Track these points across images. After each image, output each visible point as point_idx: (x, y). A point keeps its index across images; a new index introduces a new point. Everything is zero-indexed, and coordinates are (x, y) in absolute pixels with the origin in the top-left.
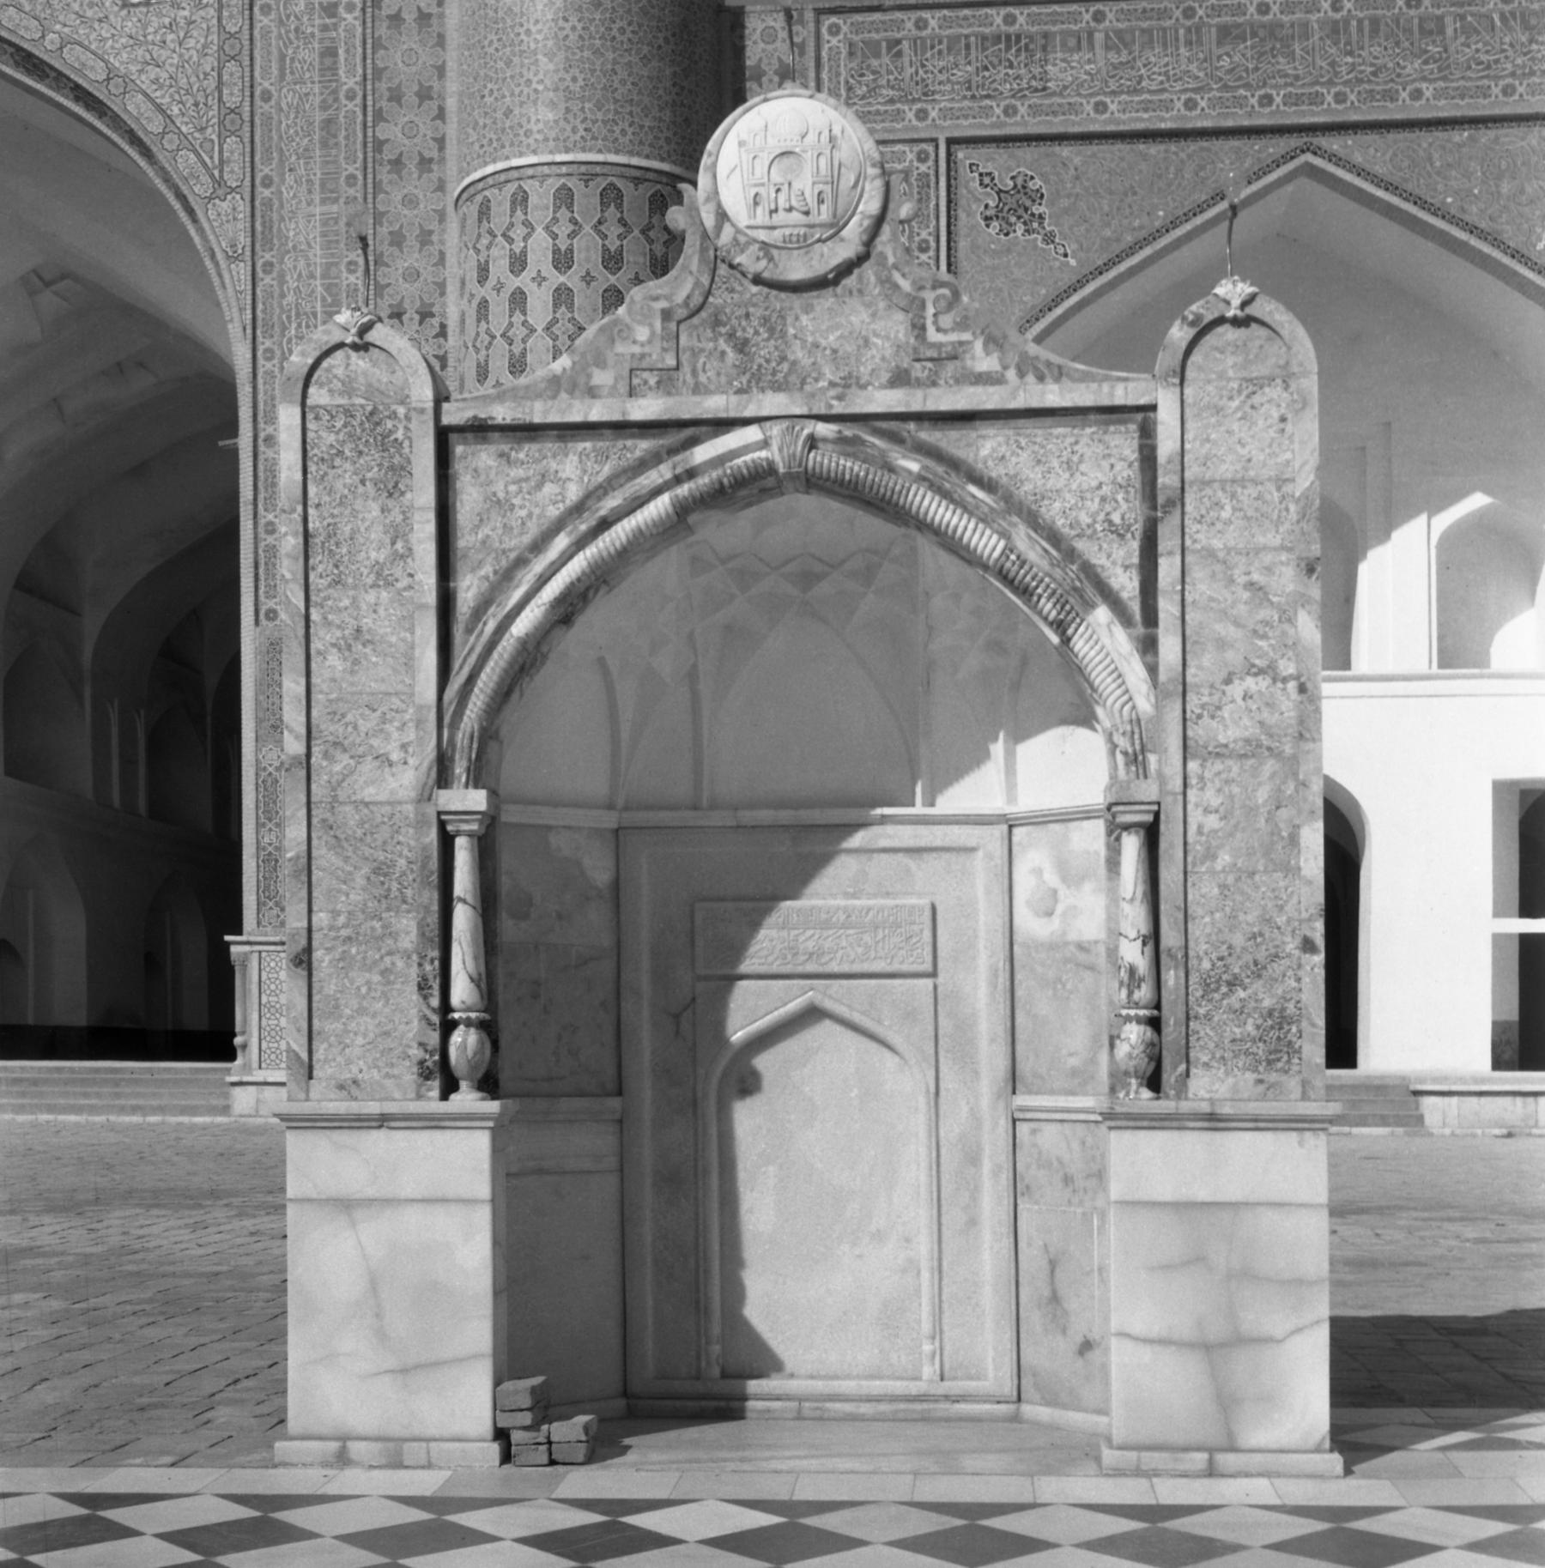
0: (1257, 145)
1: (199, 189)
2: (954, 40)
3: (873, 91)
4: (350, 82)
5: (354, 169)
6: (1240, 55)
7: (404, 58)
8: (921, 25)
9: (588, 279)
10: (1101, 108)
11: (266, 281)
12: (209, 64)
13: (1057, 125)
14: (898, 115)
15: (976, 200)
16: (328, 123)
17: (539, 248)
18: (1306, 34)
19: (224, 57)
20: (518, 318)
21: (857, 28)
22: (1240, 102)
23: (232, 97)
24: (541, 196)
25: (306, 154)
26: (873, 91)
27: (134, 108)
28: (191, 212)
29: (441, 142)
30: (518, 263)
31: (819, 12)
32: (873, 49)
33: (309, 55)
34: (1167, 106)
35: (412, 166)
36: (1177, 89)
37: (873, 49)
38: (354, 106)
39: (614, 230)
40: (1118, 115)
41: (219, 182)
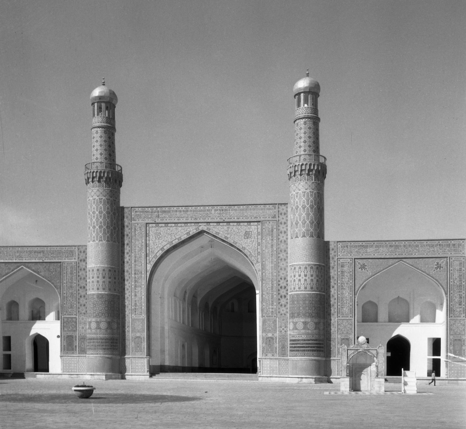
0: (395, 260)
1: (254, 262)
3: (344, 252)
4: (275, 249)
5: (276, 260)
6: (393, 249)
7: (282, 246)
8: (351, 244)
10: (374, 255)
11: (264, 274)
13: (368, 257)
15: (358, 266)
16: (272, 254)
17: (302, 274)
18: (401, 246)
19: (259, 244)
22: (392, 255)
23: (259, 251)
24: (303, 268)
25: (269, 258)
26: (344, 252)
27: (246, 251)
28: (253, 265)
29: (287, 257)
33: (270, 245)
35: (283, 260)
37: (344, 247)
39: (312, 272)
40: (376, 256)
41: (258, 261)
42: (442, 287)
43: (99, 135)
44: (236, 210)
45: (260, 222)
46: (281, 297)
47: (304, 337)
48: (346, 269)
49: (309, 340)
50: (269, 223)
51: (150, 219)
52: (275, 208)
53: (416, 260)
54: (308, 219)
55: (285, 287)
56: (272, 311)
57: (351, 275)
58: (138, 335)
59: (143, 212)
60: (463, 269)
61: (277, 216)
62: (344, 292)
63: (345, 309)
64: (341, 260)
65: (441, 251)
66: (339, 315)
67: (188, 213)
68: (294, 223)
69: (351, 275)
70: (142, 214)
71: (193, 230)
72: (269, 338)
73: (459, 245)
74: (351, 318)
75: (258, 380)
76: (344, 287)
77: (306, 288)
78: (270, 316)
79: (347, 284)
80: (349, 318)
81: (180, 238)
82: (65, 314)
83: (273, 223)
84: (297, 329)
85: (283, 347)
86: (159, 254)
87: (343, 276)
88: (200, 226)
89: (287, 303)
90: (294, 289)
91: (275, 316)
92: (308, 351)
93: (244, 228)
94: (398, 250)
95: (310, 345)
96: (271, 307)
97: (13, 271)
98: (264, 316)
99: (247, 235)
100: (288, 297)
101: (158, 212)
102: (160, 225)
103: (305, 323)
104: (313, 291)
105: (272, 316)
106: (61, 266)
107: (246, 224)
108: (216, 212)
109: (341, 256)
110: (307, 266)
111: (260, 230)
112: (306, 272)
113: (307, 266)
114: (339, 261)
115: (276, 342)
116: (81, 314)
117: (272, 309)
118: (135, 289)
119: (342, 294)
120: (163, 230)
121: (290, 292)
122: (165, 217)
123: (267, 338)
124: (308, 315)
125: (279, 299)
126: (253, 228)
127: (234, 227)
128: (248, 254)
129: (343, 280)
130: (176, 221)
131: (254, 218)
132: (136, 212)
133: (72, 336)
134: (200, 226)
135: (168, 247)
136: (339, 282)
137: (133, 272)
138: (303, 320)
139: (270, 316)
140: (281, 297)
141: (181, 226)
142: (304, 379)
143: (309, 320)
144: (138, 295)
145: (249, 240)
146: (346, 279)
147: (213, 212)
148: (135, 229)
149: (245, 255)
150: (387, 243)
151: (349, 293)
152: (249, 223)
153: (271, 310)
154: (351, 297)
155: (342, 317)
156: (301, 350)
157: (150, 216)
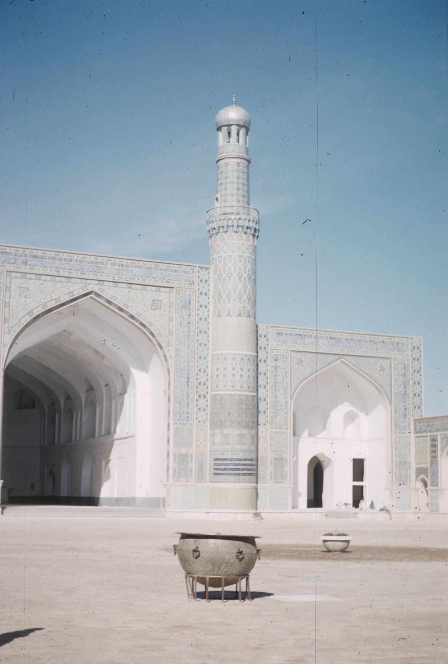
3: (279, 341)
5: (193, 344)
6: (333, 342)
14: (282, 345)
21: (276, 330)
26: (279, 341)
32: (279, 334)
33: (186, 323)
34: (323, 349)
36: (324, 346)
38: (193, 333)
41: (168, 344)
42: (386, 394)
46: (200, 396)
47: (240, 455)
48: (280, 363)
49: (245, 460)
50: (186, 291)
51: (12, 266)
53: (359, 358)
54: (245, 292)
55: (205, 384)
57: (286, 372)
60: (407, 374)
65: (385, 349)
67: (73, 263)
68: (224, 296)
71: (78, 289)
72: (181, 455)
73: (403, 345)
74: (286, 431)
76: (278, 388)
77: (242, 387)
78: (184, 424)
81: (59, 298)
84: (229, 444)
85: (201, 468)
87: (277, 373)
88: (89, 284)
89: (207, 406)
90: (225, 386)
91: (191, 424)
92: (245, 474)
93: (150, 294)
94: (339, 344)
95: (246, 467)
96: (185, 410)
99: (156, 304)
100: (209, 397)
101: (26, 256)
102: (29, 276)
103: (241, 436)
104: (250, 391)
105: (187, 424)
107: (154, 288)
108: (114, 267)
110: (244, 357)
112: (242, 364)
113: (244, 357)
114: (272, 352)
115: (192, 461)
119: (276, 396)
121: (212, 391)
122: (36, 265)
124: (244, 424)
126: (163, 295)
130: (54, 273)
134: (89, 284)
135: (40, 310)
138: (238, 432)
139: (184, 424)
140: (200, 396)
141: (61, 282)
142: (239, 515)
143: (245, 431)
147: (109, 266)
149: (151, 333)
150: (328, 333)
152: (158, 288)
153: (185, 415)
155: (276, 428)
156: (234, 474)
157: (12, 261)
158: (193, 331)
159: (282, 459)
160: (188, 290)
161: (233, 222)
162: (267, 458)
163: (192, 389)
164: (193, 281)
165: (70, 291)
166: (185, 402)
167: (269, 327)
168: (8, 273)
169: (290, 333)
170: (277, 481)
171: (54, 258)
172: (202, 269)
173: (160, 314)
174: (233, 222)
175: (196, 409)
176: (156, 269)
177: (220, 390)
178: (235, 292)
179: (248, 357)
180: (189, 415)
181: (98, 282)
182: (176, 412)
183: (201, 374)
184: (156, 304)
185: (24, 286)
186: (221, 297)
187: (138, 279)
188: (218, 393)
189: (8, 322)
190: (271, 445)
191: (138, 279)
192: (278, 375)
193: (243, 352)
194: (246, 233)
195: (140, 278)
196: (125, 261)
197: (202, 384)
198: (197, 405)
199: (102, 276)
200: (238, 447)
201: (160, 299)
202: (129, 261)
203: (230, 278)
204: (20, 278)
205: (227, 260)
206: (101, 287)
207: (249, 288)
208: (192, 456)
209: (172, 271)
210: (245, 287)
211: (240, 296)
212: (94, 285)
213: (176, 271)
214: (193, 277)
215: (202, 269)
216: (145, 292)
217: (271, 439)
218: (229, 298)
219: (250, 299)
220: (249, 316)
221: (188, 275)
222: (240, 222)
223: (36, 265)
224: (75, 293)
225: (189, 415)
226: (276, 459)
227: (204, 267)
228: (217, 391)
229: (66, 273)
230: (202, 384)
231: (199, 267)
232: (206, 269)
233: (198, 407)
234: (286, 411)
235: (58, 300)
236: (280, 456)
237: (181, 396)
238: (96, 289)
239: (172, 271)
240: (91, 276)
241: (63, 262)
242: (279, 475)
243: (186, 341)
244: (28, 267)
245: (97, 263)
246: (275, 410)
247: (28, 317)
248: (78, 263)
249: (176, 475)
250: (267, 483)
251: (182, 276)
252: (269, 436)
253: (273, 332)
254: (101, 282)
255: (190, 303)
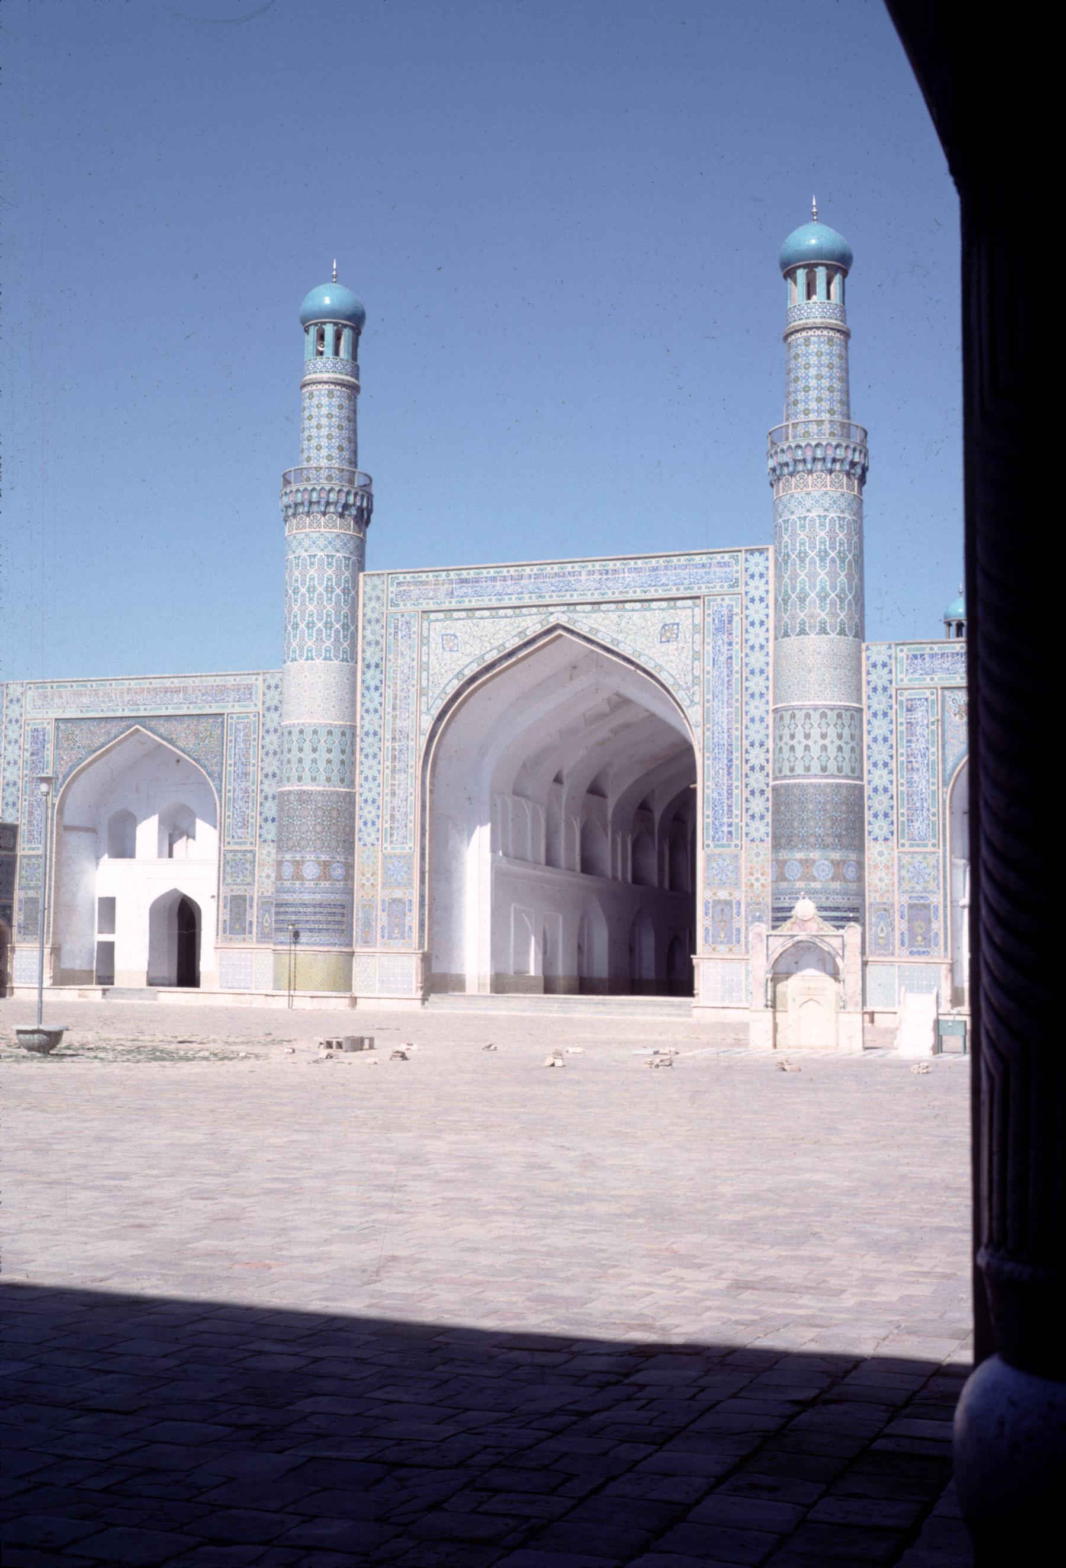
1: (685, 704)
2: (943, 655)
5: (739, 697)
9: (815, 742)
12: (689, 662)
14: (925, 679)
16: (729, 681)
19: (694, 659)
20: (792, 754)
23: (697, 673)
25: (722, 692)
30: (792, 737)
31: (897, 645)
32: (915, 657)
33: (723, 659)
37: (915, 657)
39: (824, 726)
41: (692, 701)
43: (335, 401)
44: (637, 570)
45: (698, 597)
48: (918, 715)
50: (723, 600)
51: (431, 602)
52: (737, 561)
56: (730, 833)
58: (398, 894)
59: (415, 583)
61: (742, 581)
62: (916, 778)
63: (917, 824)
64: (906, 693)
66: (901, 841)
67: (523, 582)
69: (933, 732)
70: (412, 588)
71: (532, 624)
72: (719, 901)
75: (156, 999)
76: (916, 765)
78: (722, 846)
79: (924, 755)
80: (930, 849)
81: (503, 645)
82: (229, 843)
83: (731, 599)
86: (451, 691)
87: (912, 735)
88: (552, 613)
91: (736, 846)
93: (659, 615)
96: (725, 820)
97: (115, 737)
98: (708, 846)
99: (668, 633)
101: (451, 582)
102: (456, 615)
105: (729, 846)
106: (222, 722)
107: (664, 604)
108: (591, 577)
109: (906, 683)
111: (698, 620)
115: (738, 914)
116: (265, 841)
117: (730, 825)
118: (394, 779)
119: (910, 782)
120: (460, 626)
121: (775, 779)
123: (717, 903)
125: (747, 801)
126: (685, 615)
127: (635, 616)
128: (669, 683)
129: (913, 745)
131: (685, 589)
132: (399, 584)
133: (243, 898)
134: (552, 613)
135: (475, 668)
136: (900, 751)
137: (389, 736)
140: (752, 793)
141: (506, 617)
144: (400, 793)
145: (672, 647)
146: (919, 745)
148: (396, 627)
149: (663, 685)
151: (928, 781)
152: (672, 603)
153: (725, 829)
154: (933, 792)
155: (912, 846)
157: (431, 594)
158: (737, 672)
159: (926, 907)
160: (726, 598)
161: (804, 453)
162: (893, 905)
163: (737, 779)
164: (737, 579)
165: (520, 629)
166: (725, 805)
167: (893, 646)
168: (425, 615)
169: (940, 652)
170: (915, 949)
171: (494, 579)
172: (752, 554)
173: (676, 650)
174: (804, 453)
175: (746, 818)
176: (666, 568)
177: (785, 777)
178: (813, 586)
179: (836, 712)
180: (733, 829)
181: (565, 608)
182: (708, 824)
183: (755, 751)
184: (668, 633)
185: (448, 632)
186: (789, 598)
187: (635, 592)
188: (792, 781)
189: (427, 695)
190: (901, 879)
191: (656, 591)
192: (914, 739)
193: (843, 703)
194: (831, 472)
195: (638, 590)
196: (611, 563)
197: (757, 768)
198: (747, 810)
199: (571, 596)
200: (836, 885)
201: (677, 621)
202: (618, 563)
203: (802, 561)
204: (613, 611)
205: (817, 525)
206: (571, 615)
207: (842, 577)
208: (739, 904)
209: (696, 566)
210: (833, 575)
211: (823, 594)
212: (560, 615)
213: (703, 566)
214: (737, 572)
215: (752, 554)
216: (648, 613)
217: (901, 867)
218: (802, 600)
219: (827, 596)
220: (842, 632)
221: (728, 569)
222: (838, 451)
223: (466, 595)
224: (528, 632)
225: (733, 829)
226: (911, 907)
227: (758, 550)
228: (790, 777)
229: (555, 598)
230: (757, 768)
231: (746, 551)
232: (761, 551)
233: (750, 813)
234: (934, 810)
235: (501, 648)
236: (922, 901)
237: (716, 794)
238: (563, 620)
239: (696, 566)
240: (555, 600)
241: (509, 582)
242: (919, 938)
243: (725, 692)
244: (454, 601)
245: (564, 576)
246: (908, 809)
247: (455, 682)
248: (532, 580)
249: (710, 939)
250: (893, 954)
251: (715, 573)
252: (896, 862)
253: (903, 655)
254: (572, 607)
255: (730, 622)
